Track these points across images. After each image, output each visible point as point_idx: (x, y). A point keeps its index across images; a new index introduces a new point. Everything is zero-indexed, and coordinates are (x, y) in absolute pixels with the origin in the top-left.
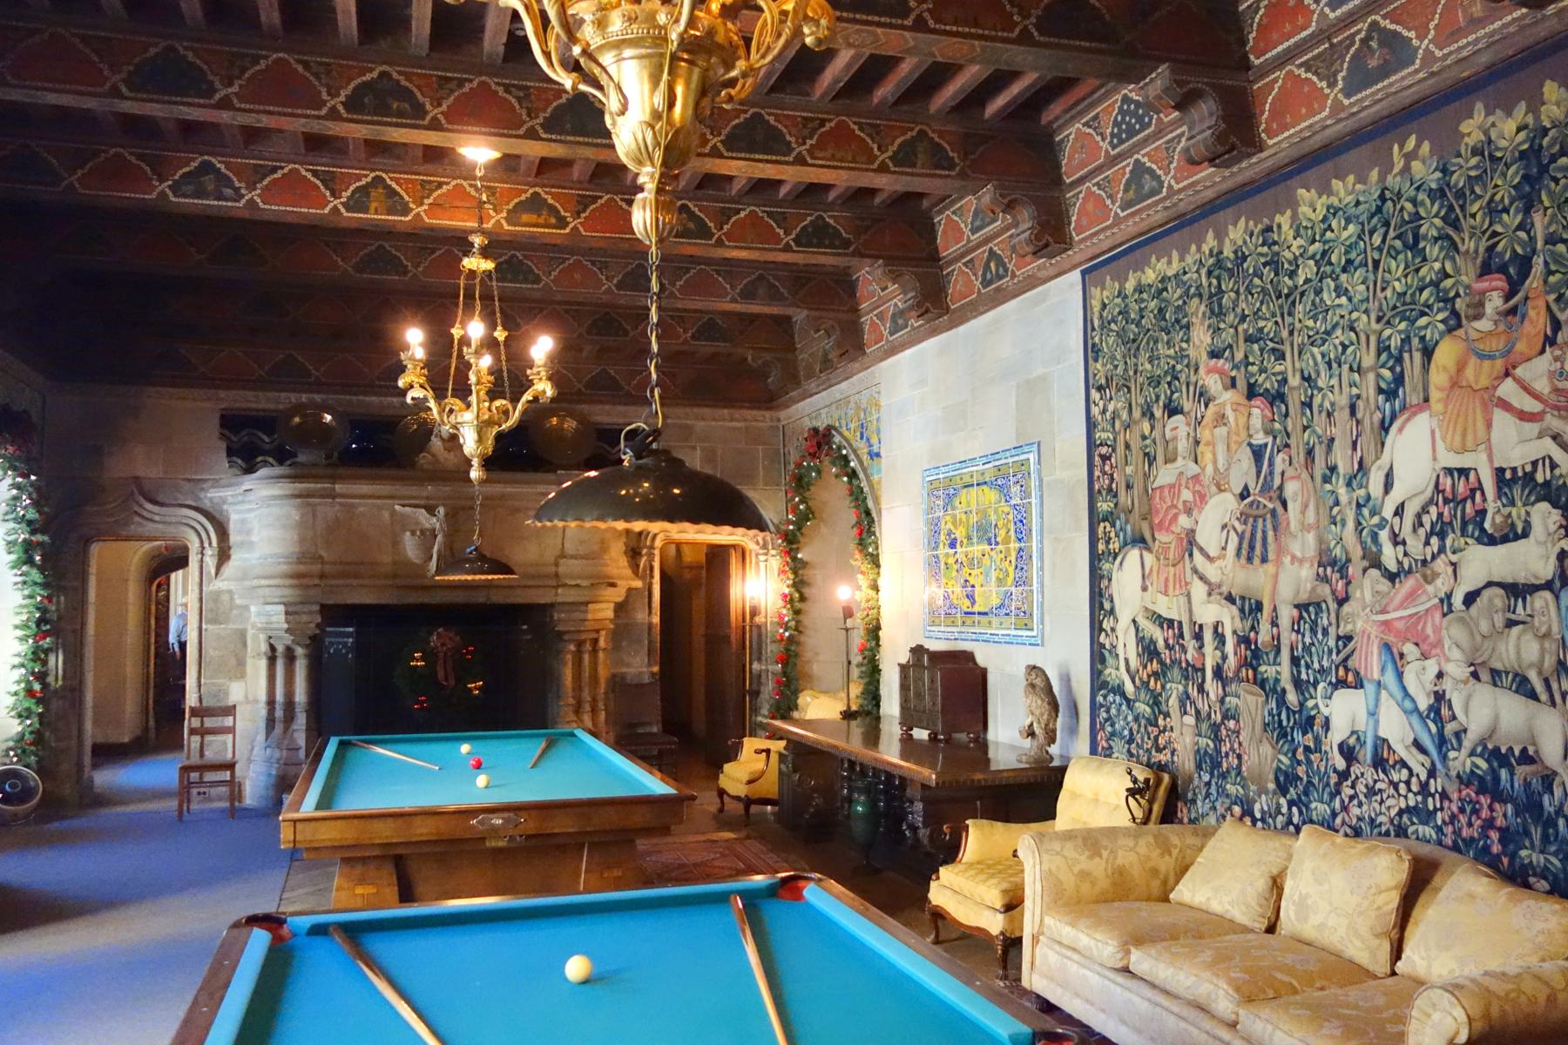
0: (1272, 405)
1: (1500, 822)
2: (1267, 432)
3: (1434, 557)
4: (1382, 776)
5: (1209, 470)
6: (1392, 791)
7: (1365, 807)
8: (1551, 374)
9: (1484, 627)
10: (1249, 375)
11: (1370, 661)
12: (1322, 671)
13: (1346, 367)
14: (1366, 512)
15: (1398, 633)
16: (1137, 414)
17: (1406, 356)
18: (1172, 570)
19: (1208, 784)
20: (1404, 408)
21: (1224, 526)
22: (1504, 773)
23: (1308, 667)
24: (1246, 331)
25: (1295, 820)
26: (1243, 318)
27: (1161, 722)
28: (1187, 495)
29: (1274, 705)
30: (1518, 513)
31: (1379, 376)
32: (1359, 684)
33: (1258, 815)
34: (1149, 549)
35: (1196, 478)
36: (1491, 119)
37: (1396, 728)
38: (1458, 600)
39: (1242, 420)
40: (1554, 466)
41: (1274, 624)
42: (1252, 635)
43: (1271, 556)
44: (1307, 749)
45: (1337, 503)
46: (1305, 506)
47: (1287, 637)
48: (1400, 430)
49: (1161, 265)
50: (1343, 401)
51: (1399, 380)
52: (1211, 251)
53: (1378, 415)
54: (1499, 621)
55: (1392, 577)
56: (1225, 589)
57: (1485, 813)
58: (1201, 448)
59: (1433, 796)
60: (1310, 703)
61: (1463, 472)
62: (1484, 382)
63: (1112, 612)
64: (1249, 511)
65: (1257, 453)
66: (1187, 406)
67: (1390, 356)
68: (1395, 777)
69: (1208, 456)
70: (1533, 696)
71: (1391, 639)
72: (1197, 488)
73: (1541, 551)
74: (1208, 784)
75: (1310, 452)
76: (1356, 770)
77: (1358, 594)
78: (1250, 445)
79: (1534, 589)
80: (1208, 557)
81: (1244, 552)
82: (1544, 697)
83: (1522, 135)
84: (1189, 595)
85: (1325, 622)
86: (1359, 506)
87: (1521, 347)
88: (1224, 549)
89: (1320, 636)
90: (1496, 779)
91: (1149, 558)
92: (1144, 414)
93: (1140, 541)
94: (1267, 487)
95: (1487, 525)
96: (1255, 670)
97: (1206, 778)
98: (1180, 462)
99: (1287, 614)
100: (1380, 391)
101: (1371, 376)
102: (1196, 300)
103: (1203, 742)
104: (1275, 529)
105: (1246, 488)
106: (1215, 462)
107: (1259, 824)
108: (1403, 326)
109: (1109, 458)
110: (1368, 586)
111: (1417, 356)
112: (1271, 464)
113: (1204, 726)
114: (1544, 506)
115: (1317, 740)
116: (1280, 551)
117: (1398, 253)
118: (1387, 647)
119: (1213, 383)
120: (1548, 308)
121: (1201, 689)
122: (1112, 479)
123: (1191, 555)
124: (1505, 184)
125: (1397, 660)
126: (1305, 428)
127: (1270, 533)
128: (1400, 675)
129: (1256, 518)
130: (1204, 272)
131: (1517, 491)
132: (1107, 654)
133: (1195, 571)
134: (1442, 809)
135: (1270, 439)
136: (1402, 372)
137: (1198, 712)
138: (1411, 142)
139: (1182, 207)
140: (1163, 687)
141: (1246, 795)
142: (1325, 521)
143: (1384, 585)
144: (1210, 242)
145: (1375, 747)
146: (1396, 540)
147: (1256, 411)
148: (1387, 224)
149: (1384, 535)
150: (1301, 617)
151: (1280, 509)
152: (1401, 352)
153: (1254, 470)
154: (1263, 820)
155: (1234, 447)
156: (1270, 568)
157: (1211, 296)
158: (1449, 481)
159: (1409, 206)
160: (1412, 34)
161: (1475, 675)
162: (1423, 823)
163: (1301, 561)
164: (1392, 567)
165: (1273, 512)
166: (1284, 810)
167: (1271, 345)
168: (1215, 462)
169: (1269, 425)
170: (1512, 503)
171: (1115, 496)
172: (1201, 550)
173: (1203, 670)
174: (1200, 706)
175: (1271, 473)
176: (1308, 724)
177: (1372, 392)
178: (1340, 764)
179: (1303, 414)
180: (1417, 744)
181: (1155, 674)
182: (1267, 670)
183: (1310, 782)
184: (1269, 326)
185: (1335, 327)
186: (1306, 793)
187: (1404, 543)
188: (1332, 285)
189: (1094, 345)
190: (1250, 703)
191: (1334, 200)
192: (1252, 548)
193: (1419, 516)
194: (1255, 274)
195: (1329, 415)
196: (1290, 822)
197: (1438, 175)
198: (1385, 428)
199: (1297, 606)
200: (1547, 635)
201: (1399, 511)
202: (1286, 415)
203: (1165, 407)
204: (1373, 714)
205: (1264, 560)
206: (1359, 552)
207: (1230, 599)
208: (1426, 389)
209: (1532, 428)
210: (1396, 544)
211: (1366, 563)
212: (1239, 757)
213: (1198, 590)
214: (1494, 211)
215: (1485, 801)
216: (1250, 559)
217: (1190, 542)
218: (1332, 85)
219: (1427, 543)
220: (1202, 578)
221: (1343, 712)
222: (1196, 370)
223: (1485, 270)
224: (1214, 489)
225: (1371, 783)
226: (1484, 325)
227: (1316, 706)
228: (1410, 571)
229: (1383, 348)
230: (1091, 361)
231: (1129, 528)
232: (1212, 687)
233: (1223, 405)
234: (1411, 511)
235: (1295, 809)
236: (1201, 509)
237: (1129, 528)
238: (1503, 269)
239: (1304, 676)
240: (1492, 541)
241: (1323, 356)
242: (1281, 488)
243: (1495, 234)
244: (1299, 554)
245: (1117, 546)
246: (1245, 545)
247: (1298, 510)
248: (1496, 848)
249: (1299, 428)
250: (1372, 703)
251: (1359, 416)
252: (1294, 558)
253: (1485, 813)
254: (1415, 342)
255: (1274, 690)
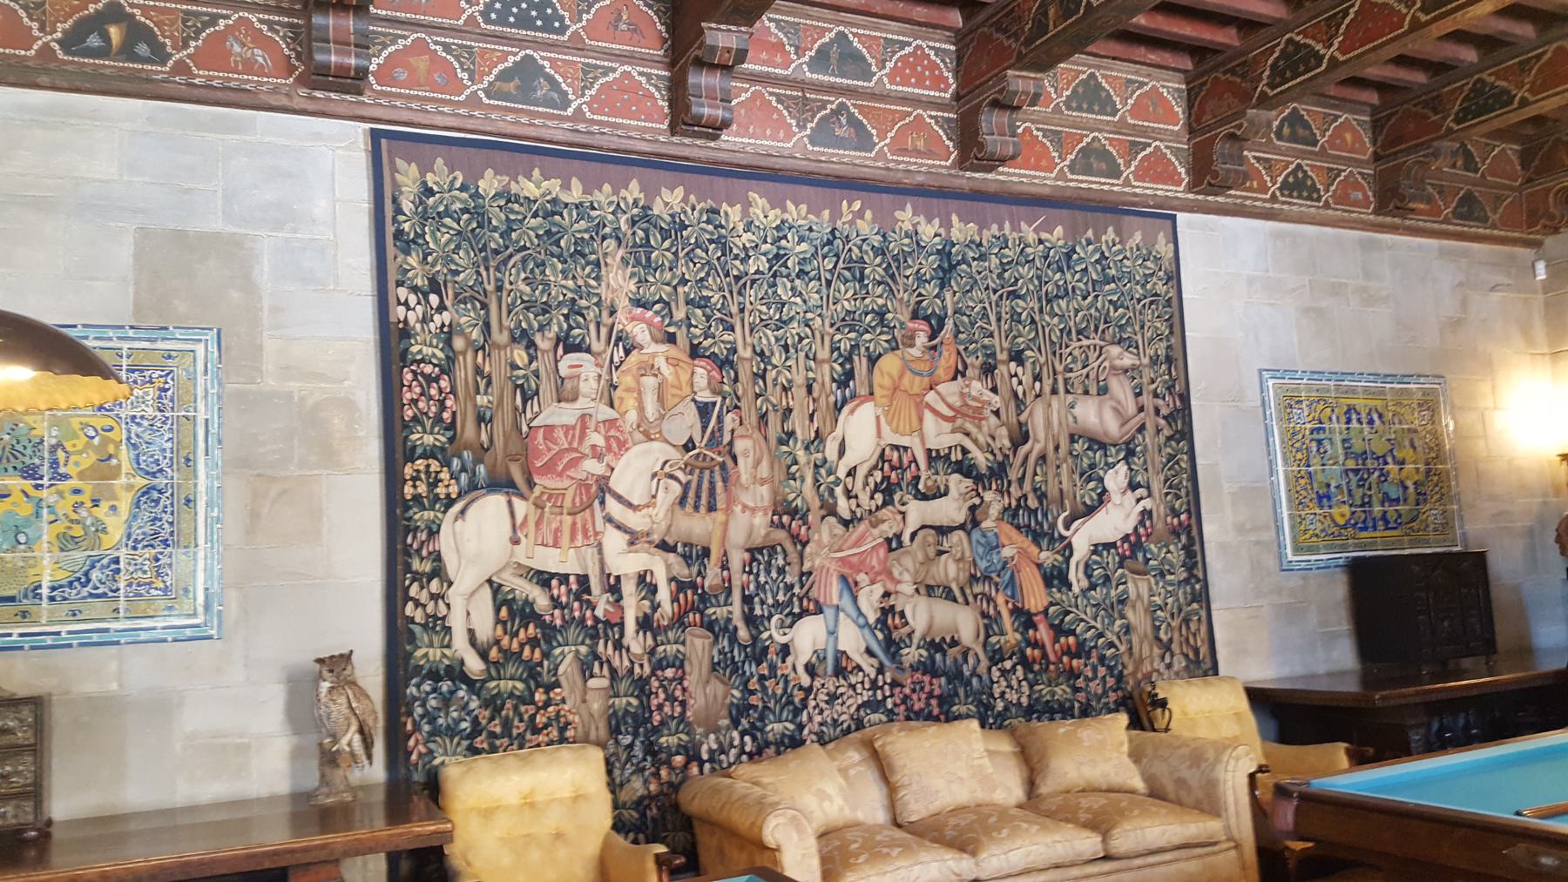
0: (721, 368)
1: (937, 692)
2: (714, 392)
3: (878, 508)
4: (842, 682)
5: (632, 416)
6: (851, 692)
7: (826, 713)
8: (962, 395)
9: (920, 556)
10: (691, 337)
11: (832, 592)
12: (777, 604)
13: (802, 355)
14: (823, 471)
15: (851, 566)
16: (501, 337)
17: (856, 358)
18: (568, 520)
19: (631, 746)
20: (854, 396)
21: (654, 475)
22: (938, 657)
23: (763, 603)
24: (687, 294)
25: (748, 749)
26: (684, 282)
27: (539, 696)
28: (597, 439)
29: (726, 643)
30: (941, 479)
31: (832, 368)
32: (819, 610)
33: (705, 757)
34: (522, 497)
35: (611, 423)
36: (917, 219)
37: (852, 640)
38: (906, 538)
39: (684, 377)
40: (965, 451)
41: (725, 566)
42: (699, 580)
43: (721, 504)
44: (762, 678)
45: (796, 463)
46: (757, 463)
47: (738, 579)
48: (852, 412)
49: (554, 186)
50: (799, 379)
51: (850, 375)
52: (636, 202)
53: (832, 399)
54: (931, 551)
55: (846, 524)
56: (656, 538)
57: (927, 689)
58: (617, 394)
59: (881, 688)
60: (765, 635)
61: (906, 448)
62: (916, 390)
63: (438, 572)
64: (692, 461)
65: (704, 410)
66: (596, 347)
67: (840, 355)
68: (853, 680)
69: (630, 403)
70: (955, 600)
71: (846, 571)
72: (612, 433)
73: (956, 505)
74: (631, 746)
75: (763, 417)
76: (817, 684)
77: (816, 537)
78: (694, 400)
79: (951, 529)
80: (630, 505)
81: (704, 500)
82: (960, 599)
83: (937, 239)
84: (600, 545)
85: (781, 562)
86: (816, 466)
87: (941, 372)
88: (654, 497)
89: (774, 575)
90: (933, 661)
91: (521, 507)
92: (514, 340)
93: (501, 483)
94: (714, 441)
95: (921, 487)
96: (702, 613)
97: (627, 740)
98: (582, 403)
99: (737, 559)
100: (834, 380)
101: (826, 367)
102: (611, 244)
103: (620, 702)
104: (725, 480)
105: (691, 440)
106: (641, 409)
107: (707, 766)
108: (853, 335)
109: (437, 379)
110: (825, 532)
111: (864, 360)
112: (720, 420)
113: (623, 686)
114: (957, 476)
115: (773, 668)
116: (731, 501)
117: (847, 281)
118: (843, 578)
119: (640, 333)
120: (959, 353)
121: (618, 645)
122: (442, 405)
123: (602, 503)
124: (929, 264)
125: (850, 587)
126: (758, 396)
127: (719, 485)
128: (855, 599)
129: (702, 470)
130: (623, 219)
131: (940, 465)
132: (417, 629)
133: (609, 519)
134: (892, 696)
135: (719, 399)
136: (852, 369)
137: (613, 671)
138: (857, 205)
139: (597, 140)
140: (546, 655)
141: (692, 741)
142: (780, 475)
143: (839, 529)
144: (633, 191)
145: (837, 661)
146: (849, 494)
147: (699, 370)
148: (837, 256)
149: (839, 490)
150: (753, 559)
151: (730, 463)
152: (851, 353)
153: (699, 425)
154: (711, 760)
155: (670, 401)
156: (719, 516)
157: (635, 245)
158: (896, 454)
159: (855, 249)
160: (874, 132)
161: (917, 590)
162: (874, 712)
163: (754, 510)
164: (846, 515)
165: (723, 466)
166: (736, 742)
167: (719, 315)
168: (641, 409)
169: (718, 387)
170: (937, 473)
171: (452, 426)
172: (619, 498)
173: (622, 625)
174: (616, 663)
175: (721, 429)
176: (759, 655)
177: (827, 379)
178: (805, 680)
179: (755, 383)
180: (869, 652)
181: (533, 642)
182: (717, 612)
183: (766, 708)
184: (716, 297)
185: (792, 319)
186: (762, 718)
187: (856, 497)
188: (789, 285)
189: (399, 234)
190: (698, 646)
191: (786, 216)
192: (698, 497)
193: (866, 477)
194: (697, 245)
195: (785, 389)
196: (743, 752)
197: (879, 238)
198: (838, 408)
199: (748, 550)
200: (961, 559)
201: (852, 473)
202: (736, 380)
203: (558, 339)
204: (832, 633)
205: (712, 508)
206: (818, 503)
207: (664, 546)
208: (871, 386)
209: (947, 426)
210: (849, 498)
211: (823, 512)
212: (683, 704)
213: (614, 541)
214: (920, 279)
215: (927, 679)
216: (696, 508)
217: (603, 488)
218: (802, 127)
219: (872, 498)
220: (619, 527)
221: (808, 637)
222: (612, 313)
223: (915, 316)
224: (638, 436)
225: (832, 689)
226: (915, 352)
227: (770, 637)
228: (861, 519)
229: (834, 348)
230: (391, 250)
231: (481, 469)
232: (636, 643)
233: (654, 355)
234: (861, 473)
235: (747, 738)
236: (618, 456)
237: (481, 469)
238: (927, 319)
239: (758, 612)
240: (925, 497)
241: (777, 340)
242: (731, 444)
243: (920, 295)
244: (751, 504)
245: (454, 490)
246: (691, 494)
247: (750, 465)
248: (936, 711)
249: (751, 395)
250: (831, 624)
251: (815, 395)
252: (745, 507)
253: (927, 689)
254: (863, 350)
255: (725, 629)
